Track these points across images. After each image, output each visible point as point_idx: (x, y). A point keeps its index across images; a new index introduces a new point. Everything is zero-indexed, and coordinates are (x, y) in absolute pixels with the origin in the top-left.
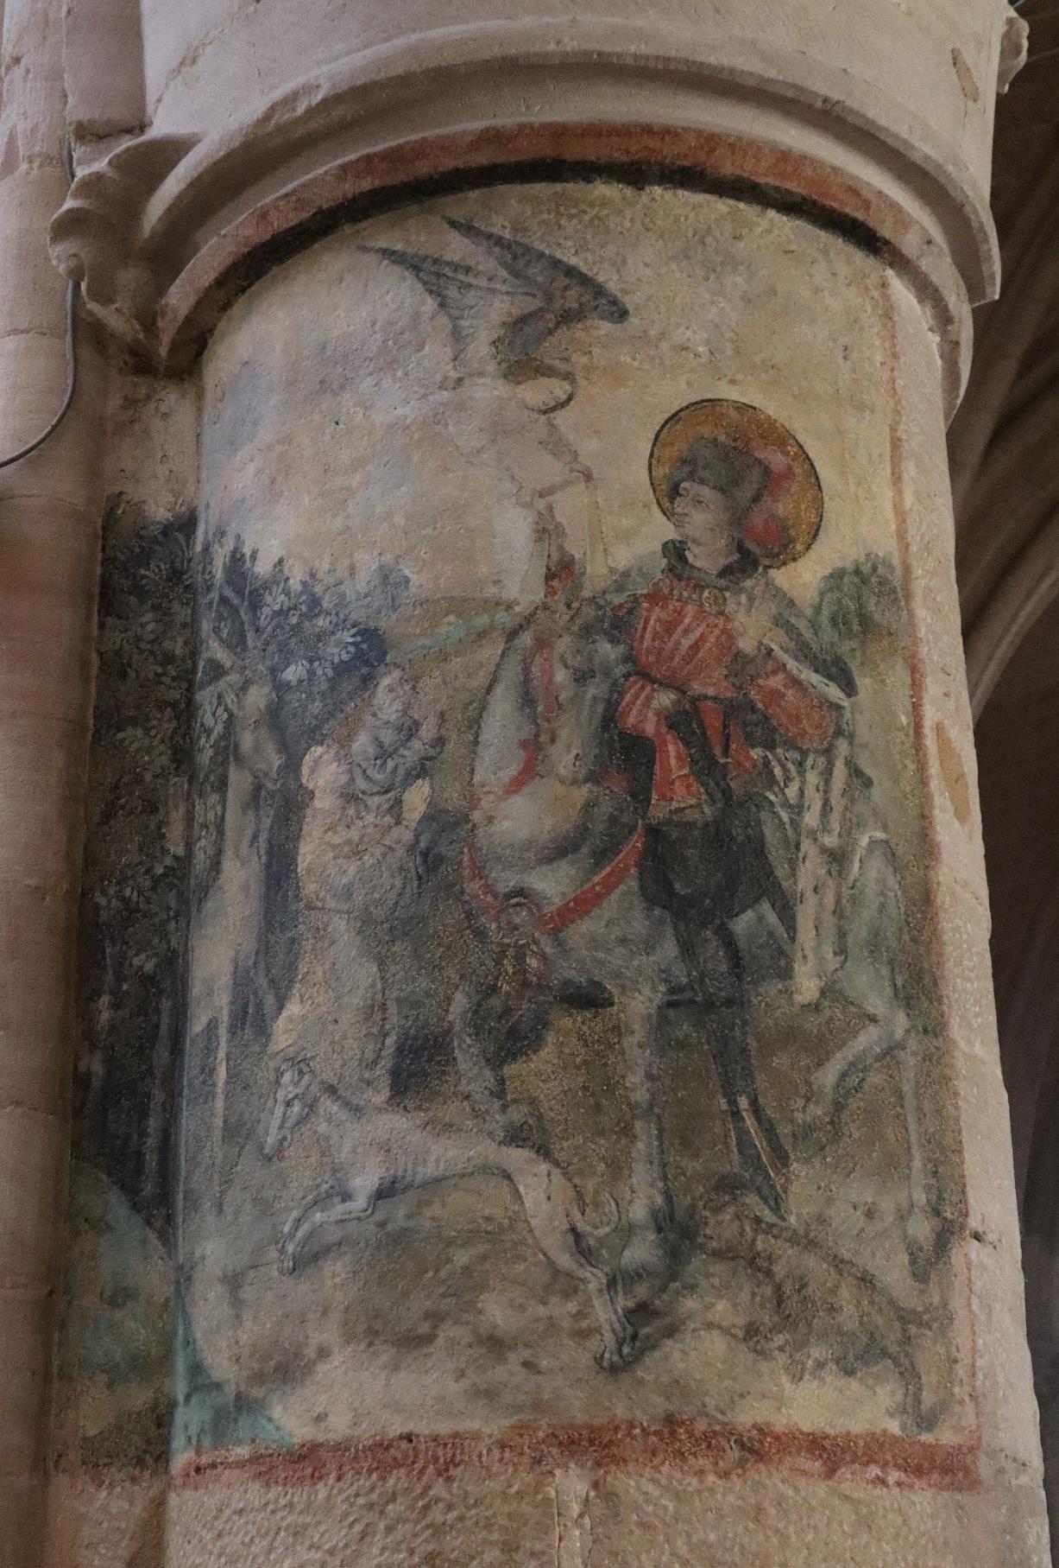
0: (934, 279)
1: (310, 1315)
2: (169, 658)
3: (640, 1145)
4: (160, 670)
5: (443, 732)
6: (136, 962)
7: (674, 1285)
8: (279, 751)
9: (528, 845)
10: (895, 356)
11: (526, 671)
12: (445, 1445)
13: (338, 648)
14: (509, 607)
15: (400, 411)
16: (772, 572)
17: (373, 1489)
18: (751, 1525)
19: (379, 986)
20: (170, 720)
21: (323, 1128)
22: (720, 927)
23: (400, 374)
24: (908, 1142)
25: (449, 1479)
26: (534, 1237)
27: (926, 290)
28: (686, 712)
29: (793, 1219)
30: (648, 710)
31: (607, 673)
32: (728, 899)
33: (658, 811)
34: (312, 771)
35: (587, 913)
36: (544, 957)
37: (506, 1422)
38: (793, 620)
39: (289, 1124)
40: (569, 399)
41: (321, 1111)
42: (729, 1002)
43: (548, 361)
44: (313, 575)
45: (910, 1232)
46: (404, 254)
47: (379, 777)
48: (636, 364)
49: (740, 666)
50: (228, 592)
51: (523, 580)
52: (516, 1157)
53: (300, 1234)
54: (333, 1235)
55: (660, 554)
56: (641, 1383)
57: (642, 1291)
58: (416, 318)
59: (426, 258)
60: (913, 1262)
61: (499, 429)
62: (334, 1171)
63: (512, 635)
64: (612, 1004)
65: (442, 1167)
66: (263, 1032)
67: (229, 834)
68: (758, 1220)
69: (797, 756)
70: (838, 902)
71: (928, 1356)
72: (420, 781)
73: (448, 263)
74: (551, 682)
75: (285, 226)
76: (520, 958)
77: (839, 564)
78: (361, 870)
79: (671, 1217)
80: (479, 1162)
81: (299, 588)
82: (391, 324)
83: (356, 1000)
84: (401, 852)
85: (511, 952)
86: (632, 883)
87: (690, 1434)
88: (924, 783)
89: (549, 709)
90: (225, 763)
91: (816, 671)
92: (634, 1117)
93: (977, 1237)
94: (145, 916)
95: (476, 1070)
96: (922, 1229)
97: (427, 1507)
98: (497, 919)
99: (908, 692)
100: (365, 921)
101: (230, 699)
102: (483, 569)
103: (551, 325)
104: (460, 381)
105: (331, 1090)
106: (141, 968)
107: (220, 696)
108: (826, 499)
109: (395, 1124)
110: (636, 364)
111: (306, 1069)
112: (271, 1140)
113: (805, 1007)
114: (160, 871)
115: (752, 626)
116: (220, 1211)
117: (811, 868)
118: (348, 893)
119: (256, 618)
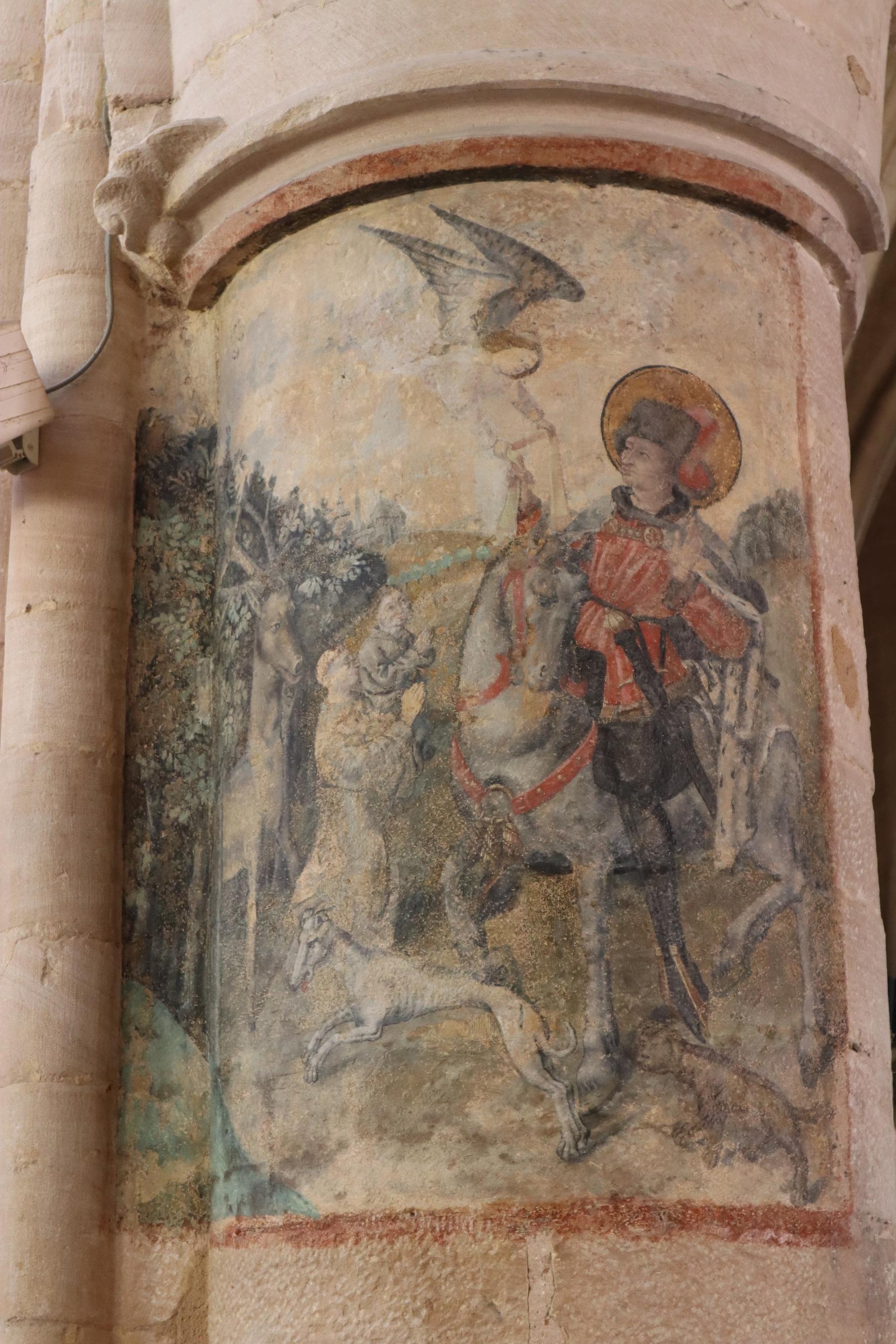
0: (834, 248)
1: (331, 1116)
2: (195, 554)
3: (593, 985)
4: (187, 565)
5: (435, 645)
6: (173, 814)
7: (618, 1095)
8: (297, 652)
9: (504, 741)
10: (801, 316)
11: (502, 596)
12: (441, 1217)
13: (346, 569)
14: (487, 543)
15: (397, 371)
16: (701, 512)
17: (383, 1250)
18: (676, 1277)
19: (384, 853)
20: (197, 608)
21: (339, 966)
22: (656, 807)
23: (396, 338)
24: (802, 976)
25: (443, 1244)
26: (509, 1057)
27: (826, 256)
28: (631, 631)
29: (711, 1042)
30: (601, 629)
31: (567, 599)
32: (664, 784)
33: (608, 713)
34: (326, 671)
35: (551, 796)
36: (516, 833)
37: (488, 1200)
38: (717, 552)
39: (311, 961)
40: (537, 366)
41: (337, 952)
42: (663, 870)
43: (518, 333)
44: (324, 505)
45: (802, 1048)
46: (399, 235)
47: (382, 680)
48: (591, 336)
49: (675, 591)
50: (249, 508)
51: (499, 520)
52: (495, 994)
53: (321, 1051)
54: (349, 1052)
55: (610, 499)
56: (592, 1170)
57: (593, 1099)
58: (408, 292)
59: (417, 240)
60: (804, 1071)
61: (478, 390)
62: (349, 1002)
63: (491, 565)
64: (571, 872)
65: (436, 1001)
66: (287, 884)
67: (254, 716)
68: (684, 1043)
69: (719, 665)
70: (750, 785)
71: (815, 1142)
72: (415, 685)
73: (436, 247)
74: (522, 605)
75: (297, 208)
76: (498, 832)
77: (755, 502)
78: (368, 755)
79: (617, 1041)
80: (465, 997)
81: (313, 515)
82: (388, 295)
83: (365, 864)
84: (400, 743)
85: (490, 829)
86: (586, 773)
87: (630, 1208)
88: (820, 679)
89: (520, 628)
90: (249, 655)
91: (736, 593)
92: (589, 962)
93: (855, 1048)
94: (179, 775)
95: (462, 924)
96: (811, 1044)
97: (425, 1266)
98: (479, 800)
99: (808, 604)
100: (372, 799)
101: (253, 601)
102: (467, 509)
103: (522, 302)
104: (446, 347)
105: (346, 936)
106: (177, 819)
107: (243, 598)
108: (744, 446)
109: (396, 965)
110: (591, 336)
111: (324, 918)
112: (296, 975)
113: (724, 872)
114: (190, 737)
115: (684, 559)
116: (253, 1027)
117: (729, 758)
118: (356, 775)
119: (274, 536)
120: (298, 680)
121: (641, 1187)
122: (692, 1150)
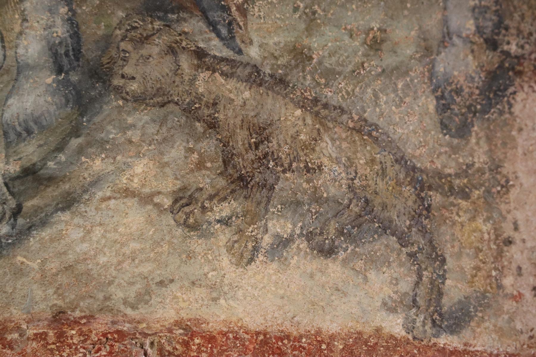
7: (75, 143)
29: (254, 53)
45: (440, 68)
57: (30, 151)
60: (444, 107)
68: (200, 54)
79: (77, 53)
121: (107, 298)
122: (206, 235)
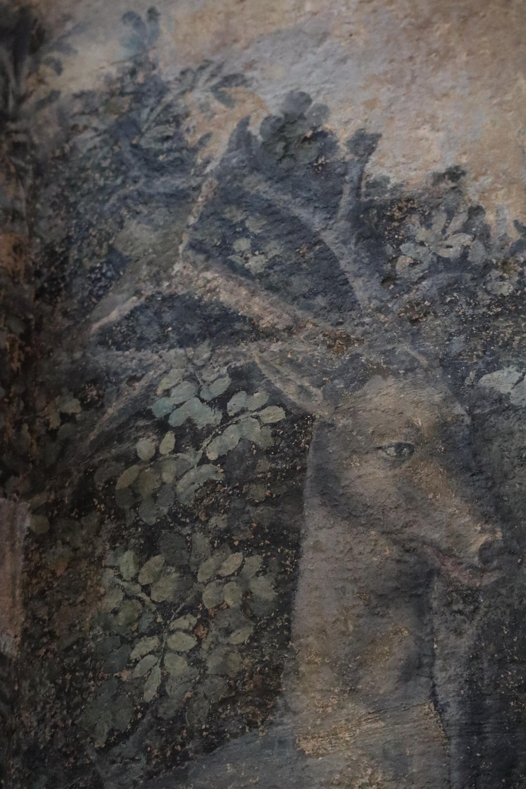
120: (489, 579)
